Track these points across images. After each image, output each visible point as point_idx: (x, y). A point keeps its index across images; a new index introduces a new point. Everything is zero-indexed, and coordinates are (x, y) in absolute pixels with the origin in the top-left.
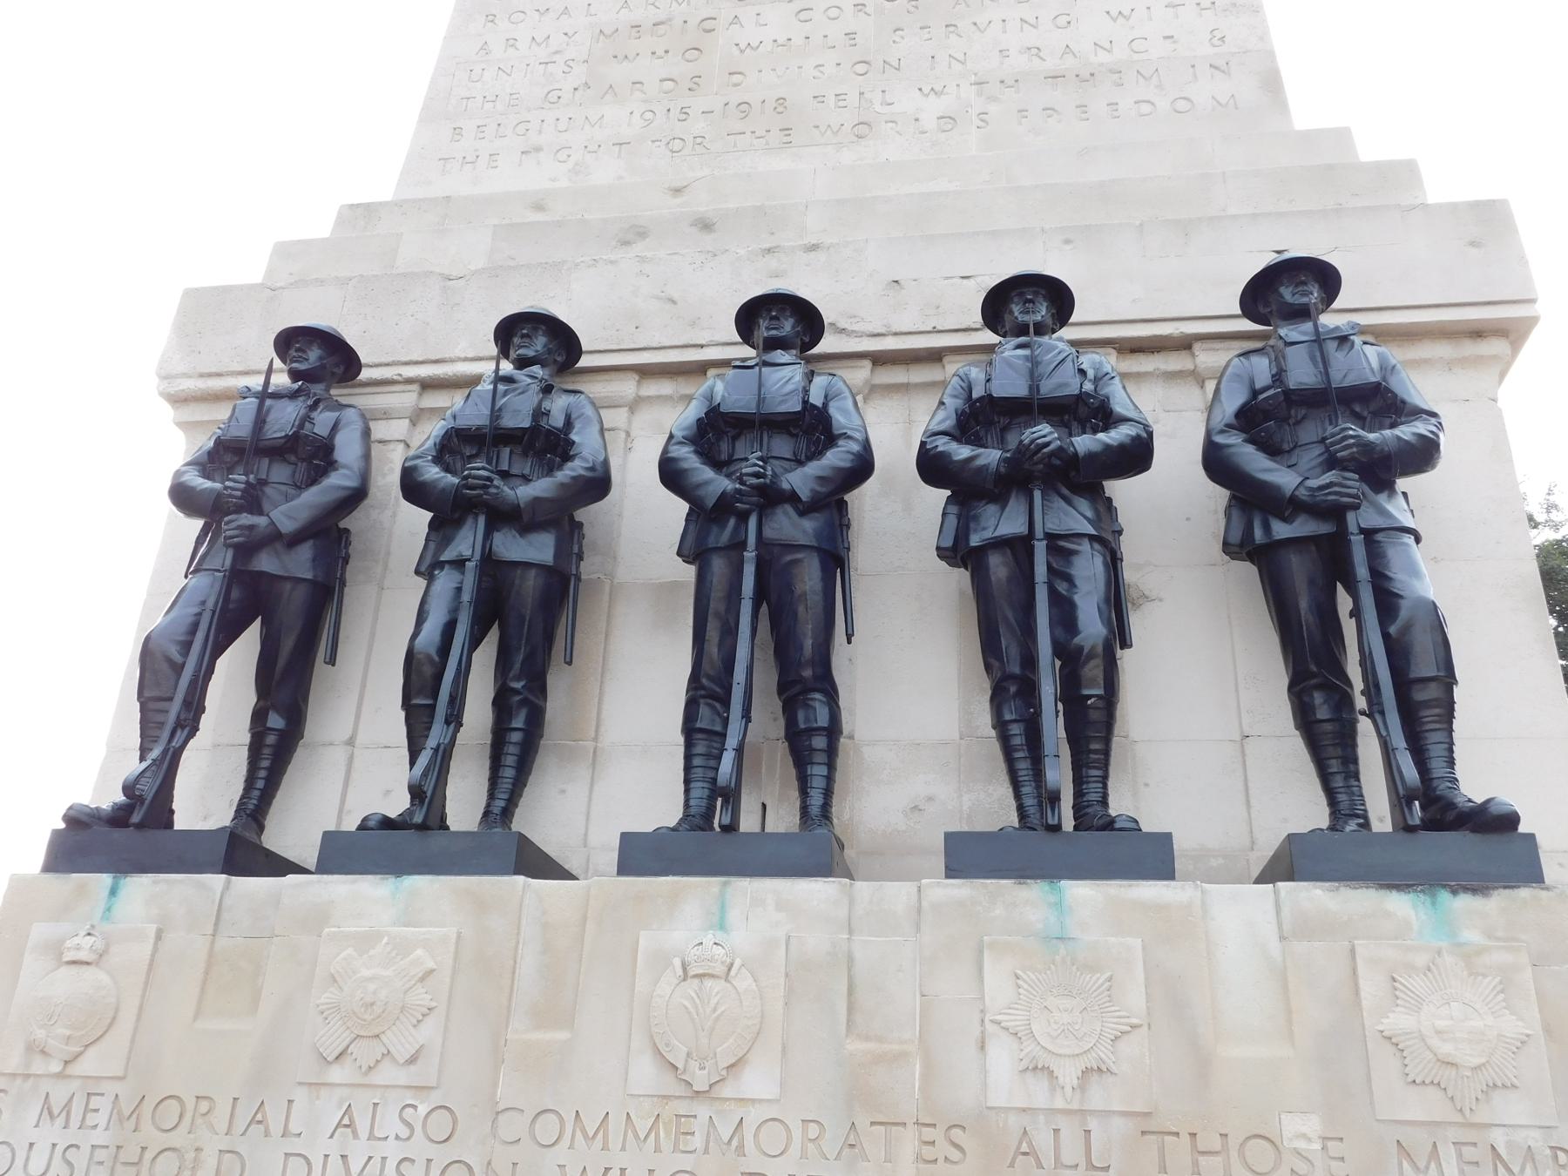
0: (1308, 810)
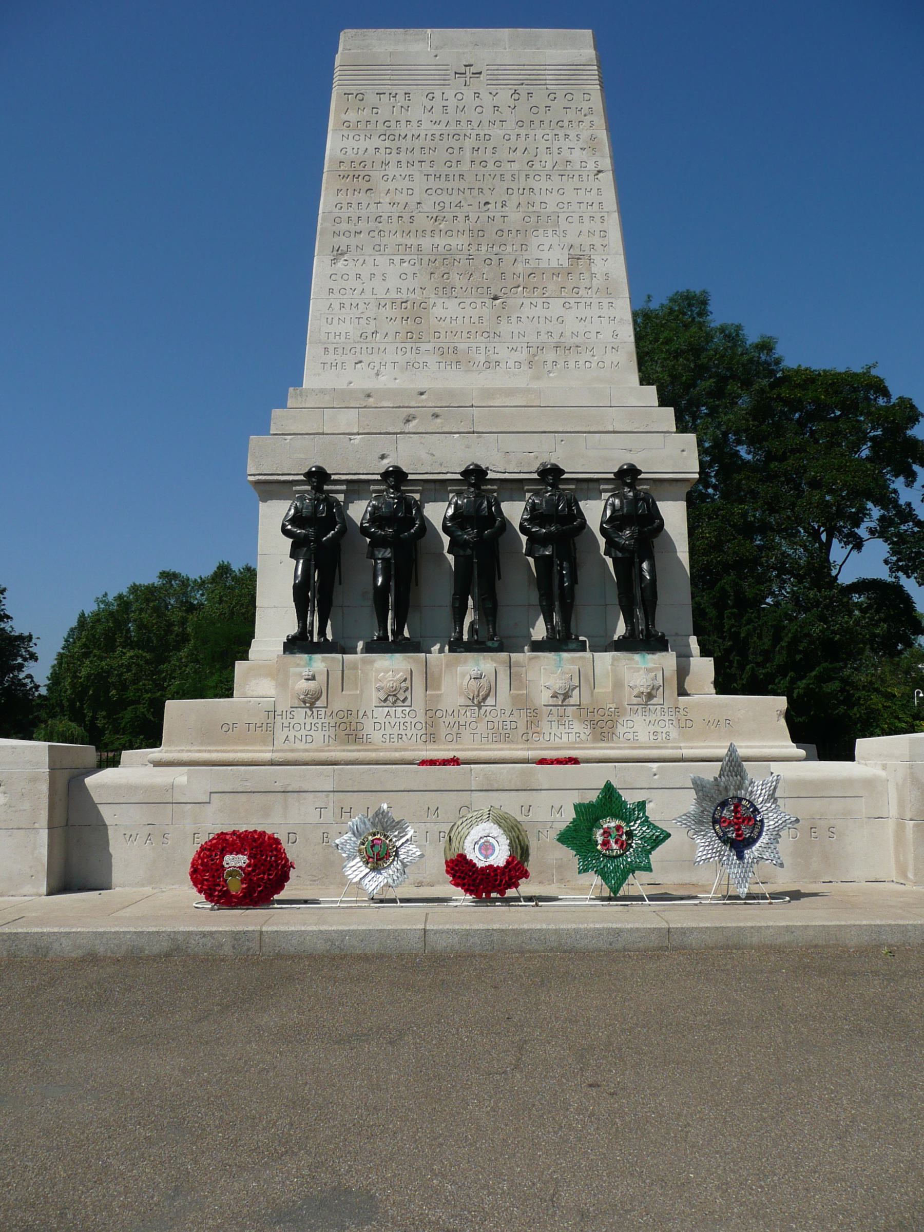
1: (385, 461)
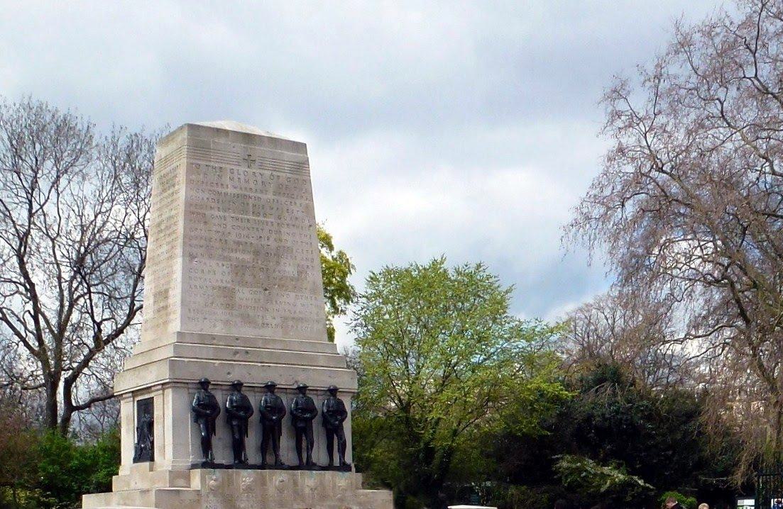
1: (229, 376)
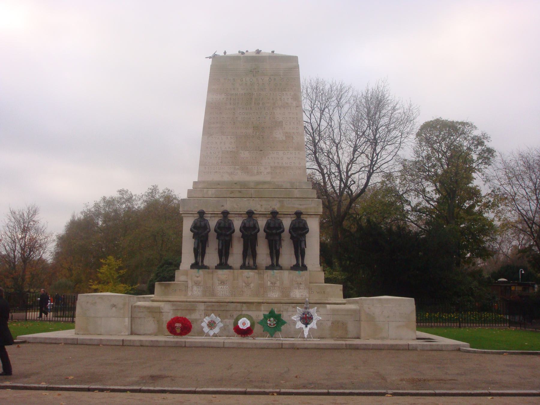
0: (294, 262)
1: (223, 208)
